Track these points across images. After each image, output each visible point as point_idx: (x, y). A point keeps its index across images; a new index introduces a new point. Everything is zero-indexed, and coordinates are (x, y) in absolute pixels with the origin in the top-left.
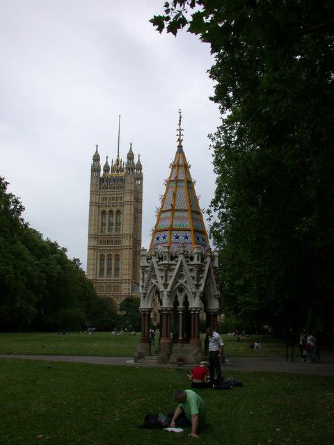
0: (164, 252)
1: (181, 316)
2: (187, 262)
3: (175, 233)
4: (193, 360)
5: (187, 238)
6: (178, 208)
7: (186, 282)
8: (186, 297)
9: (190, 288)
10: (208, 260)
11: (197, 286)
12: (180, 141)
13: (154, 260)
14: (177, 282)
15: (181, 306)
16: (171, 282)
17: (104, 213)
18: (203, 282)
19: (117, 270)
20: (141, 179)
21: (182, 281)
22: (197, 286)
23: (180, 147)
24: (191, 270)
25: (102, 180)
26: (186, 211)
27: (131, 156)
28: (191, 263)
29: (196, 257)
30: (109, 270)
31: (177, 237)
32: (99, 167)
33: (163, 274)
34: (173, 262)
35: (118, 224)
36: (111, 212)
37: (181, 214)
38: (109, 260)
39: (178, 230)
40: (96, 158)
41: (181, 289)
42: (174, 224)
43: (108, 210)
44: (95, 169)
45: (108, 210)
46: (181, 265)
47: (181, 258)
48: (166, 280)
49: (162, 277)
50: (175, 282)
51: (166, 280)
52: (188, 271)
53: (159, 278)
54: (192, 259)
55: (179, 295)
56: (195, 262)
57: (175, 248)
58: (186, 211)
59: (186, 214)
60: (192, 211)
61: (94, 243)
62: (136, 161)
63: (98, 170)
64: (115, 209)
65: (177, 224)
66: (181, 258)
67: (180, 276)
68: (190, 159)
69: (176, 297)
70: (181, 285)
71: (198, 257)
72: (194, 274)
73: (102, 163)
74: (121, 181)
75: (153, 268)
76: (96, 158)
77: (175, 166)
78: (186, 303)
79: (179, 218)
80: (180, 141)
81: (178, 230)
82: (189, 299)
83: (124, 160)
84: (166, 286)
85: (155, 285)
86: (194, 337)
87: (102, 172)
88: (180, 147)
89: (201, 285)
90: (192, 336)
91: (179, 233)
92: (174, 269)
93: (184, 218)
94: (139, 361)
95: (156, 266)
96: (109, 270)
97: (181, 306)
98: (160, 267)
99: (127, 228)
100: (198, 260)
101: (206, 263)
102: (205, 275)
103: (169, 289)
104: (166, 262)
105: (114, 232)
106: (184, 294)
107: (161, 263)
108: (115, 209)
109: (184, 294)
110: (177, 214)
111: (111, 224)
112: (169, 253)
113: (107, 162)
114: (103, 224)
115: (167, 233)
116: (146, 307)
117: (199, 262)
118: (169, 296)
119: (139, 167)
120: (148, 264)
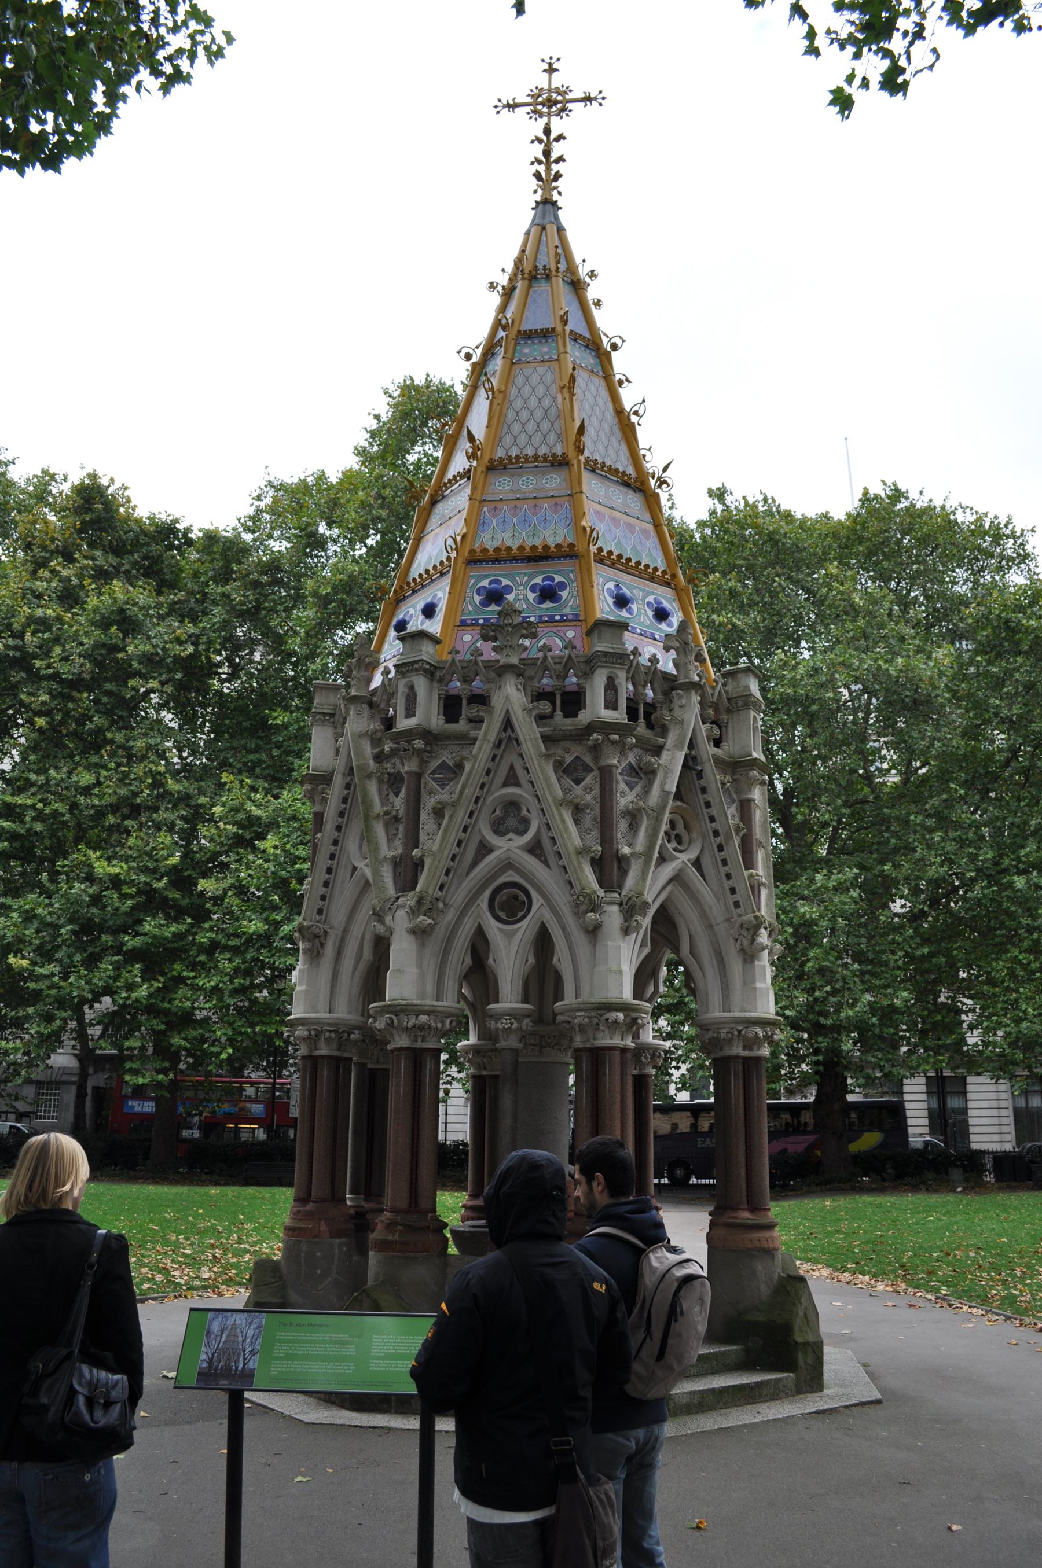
2: (541, 718)
5: (548, 594)
12: (547, 179)
15: (509, 999)
21: (509, 846)
23: (547, 206)
33: (399, 804)
37: (528, 483)
41: (511, 903)
48: (413, 840)
54: (573, 702)
68: (585, 248)
70: (509, 865)
71: (611, 686)
78: (543, 979)
80: (547, 179)
81: (501, 557)
88: (547, 206)
97: (509, 999)
106: (525, 929)
109: (525, 929)
118: (420, 934)
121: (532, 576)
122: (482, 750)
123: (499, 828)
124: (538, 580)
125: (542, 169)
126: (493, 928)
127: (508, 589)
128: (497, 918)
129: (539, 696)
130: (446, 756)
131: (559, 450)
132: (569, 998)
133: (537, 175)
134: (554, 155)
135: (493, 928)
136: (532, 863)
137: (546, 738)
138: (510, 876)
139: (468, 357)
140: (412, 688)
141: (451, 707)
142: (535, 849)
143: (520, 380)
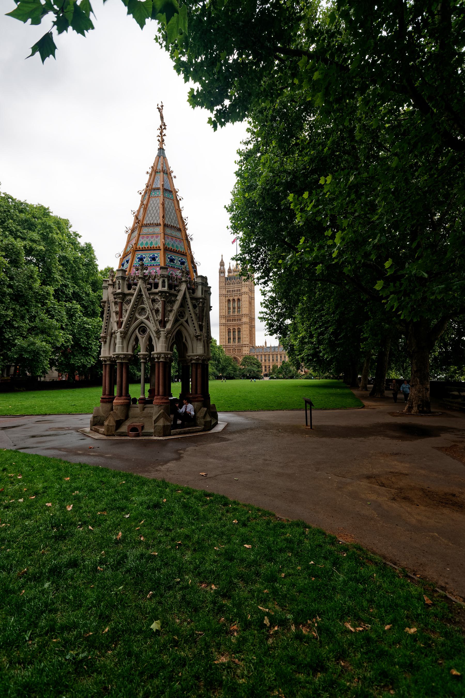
1: (142, 365)
2: (149, 290)
3: (139, 254)
4: (152, 430)
5: (154, 259)
8: (150, 339)
9: (152, 326)
10: (183, 287)
11: (163, 323)
14: (137, 319)
15: (143, 352)
17: (229, 301)
18: (171, 317)
19: (239, 338)
21: (142, 318)
22: (163, 323)
23: (161, 150)
24: (154, 301)
25: (227, 279)
28: (154, 290)
30: (234, 338)
35: (239, 308)
36: (234, 300)
37: (151, 230)
38: (234, 332)
39: (143, 250)
41: (143, 330)
42: (140, 243)
43: (231, 298)
44: (222, 272)
45: (231, 298)
46: (140, 295)
50: (132, 318)
54: (156, 286)
60: (165, 226)
61: (224, 321)
64: (236, 298)
69: (137, 340)
70: (142, 322)
71: (164, 282)
72: (159, 306)
73: (226, 268)
76: (222, 264)
77: (155, 172)
78: (150, 347)
81: (143, 250)
82: (154, 343)
86: (158, 394)
88: (161, 150)
89: (168, 321)
90: (156, 393)
91: (143, 254)
93: (153, 234)
96: (234, 338)
97: (143, 352)
99: (245, 310)
100: (163, 286)
101: (179, 291)
102: (176, 306)
105: (236, 313)
108: (236, 298)
111: (234, 308)
114: (229, 308)
117: (166, 289)
123: (140, 314)
124: (151, 256)
125: (160, 138)
127: (145, 258)
128: (140, 334)
130: (128, 298)
133: (159, 140)
134: (163, 134)
135: (139, 336)
136: (146, 321)
139: (141, 193)
142: (148, 318)
143: (151, 202)
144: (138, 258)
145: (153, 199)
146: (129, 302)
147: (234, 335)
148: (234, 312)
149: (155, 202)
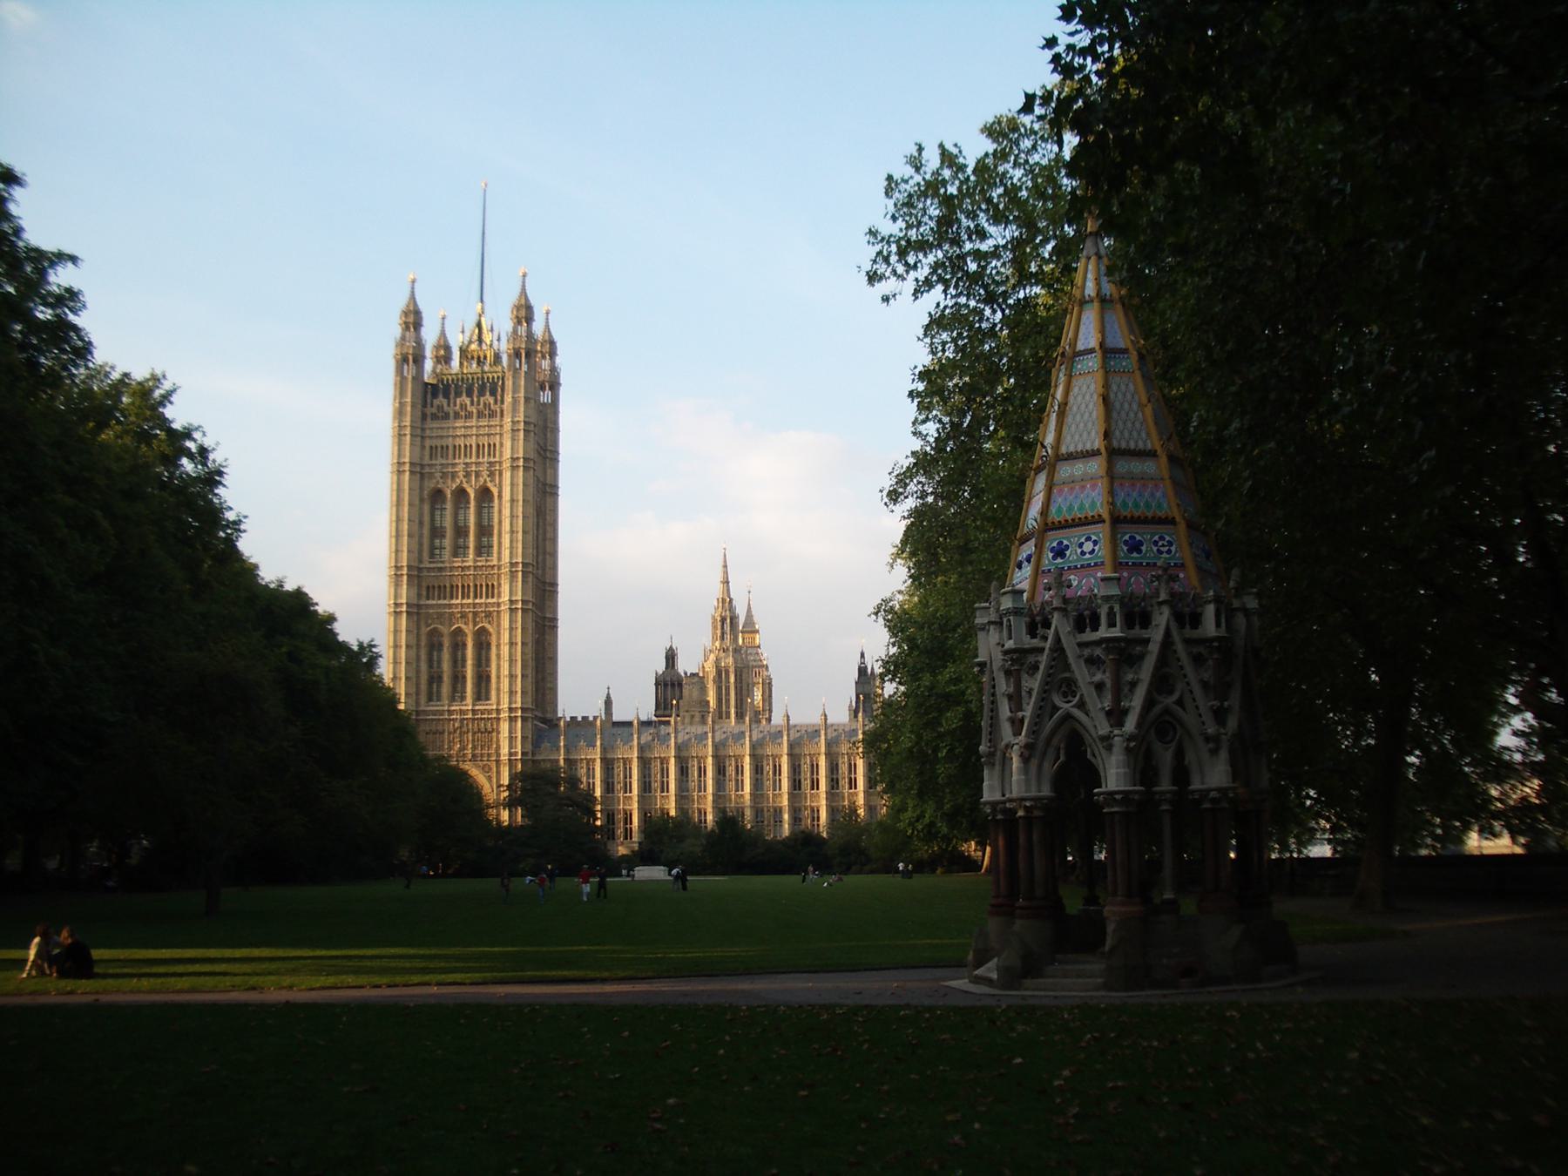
0: (1107, 598)
6: (1123, 445)
7: (1180, 702)
8: (1180, 754)
11: (1220, 715)
13: (1059, 624)
15: (1165, 785)
16: (1136, 702)
20: (554, 385)
24: (1198, 660)
26: (1152, 454)
27: (524, 312)
28: (1196, 634)
29: (1210, 610)
30: (458, 679)
31: (1135, 547)
32: (420, 345)
34: (1137, 632)
37: (1137, 466)
39: (1134, 520)
40: (413, 319)
44: (409, 357)
47: (1162, 618)
49: (1099, 687)
50: (1149, 703)
51: (1117, 698)
52: (1185, 660)
53: (1086, 691)
54: (1196, 620)
55: (1157, 746)
56: (1209, 627)
57: (1138, 584)
58: (1152, 454)
59: (1148, 467)
62: (538, 328)
63: (419, 359)
65: (1132, 501)
66: (1162, 618)
67: (1162, 682)
69: (1149, 755)
70: (1167, 711)
73: (430, 335)
74: (493, 393)
75: (1058, 648)
76: (413, 319)
78: (1181, 775)
79: (1133, 478)
81: (1134, 520)
83: (501, 324)
84: (1116, 715)
85: (1068, 717)
87: (429, 365)
92: (1141, 657)
93: (1143, 478)
94: (1028, 982)
95: (1069, 644)
97: (1165, 785)
98: (1087, 652)
100: (1218, 625)
103: (1130, 725)
104: (1103, 632)
107: (1089, 636)
110: (1122, 466)
112: (1121, 600)
113: (443, 334)
115: (1101, 532)
116: (1033, 794)
117: (1223, 632)
118: (1128, 750)
119: (551, 348)
120: (1036, 642)
121: (1153, 535)
122: (1154, 648)
126: (1157, 746)
127: (1141, 543)
129: (1178, 617)
131: (1149, 446)
132: (1196, 785)
137: (1188, 642)
138: (1167, 718)
140: (1111, 608)
141: (1129, 622)
143: (1114, 387)
144: (1126, 543)
145: (1117, 379)
146: (1134, 661)
147: (458, 662)
148: (459, 550)
149: (1123, 387)
